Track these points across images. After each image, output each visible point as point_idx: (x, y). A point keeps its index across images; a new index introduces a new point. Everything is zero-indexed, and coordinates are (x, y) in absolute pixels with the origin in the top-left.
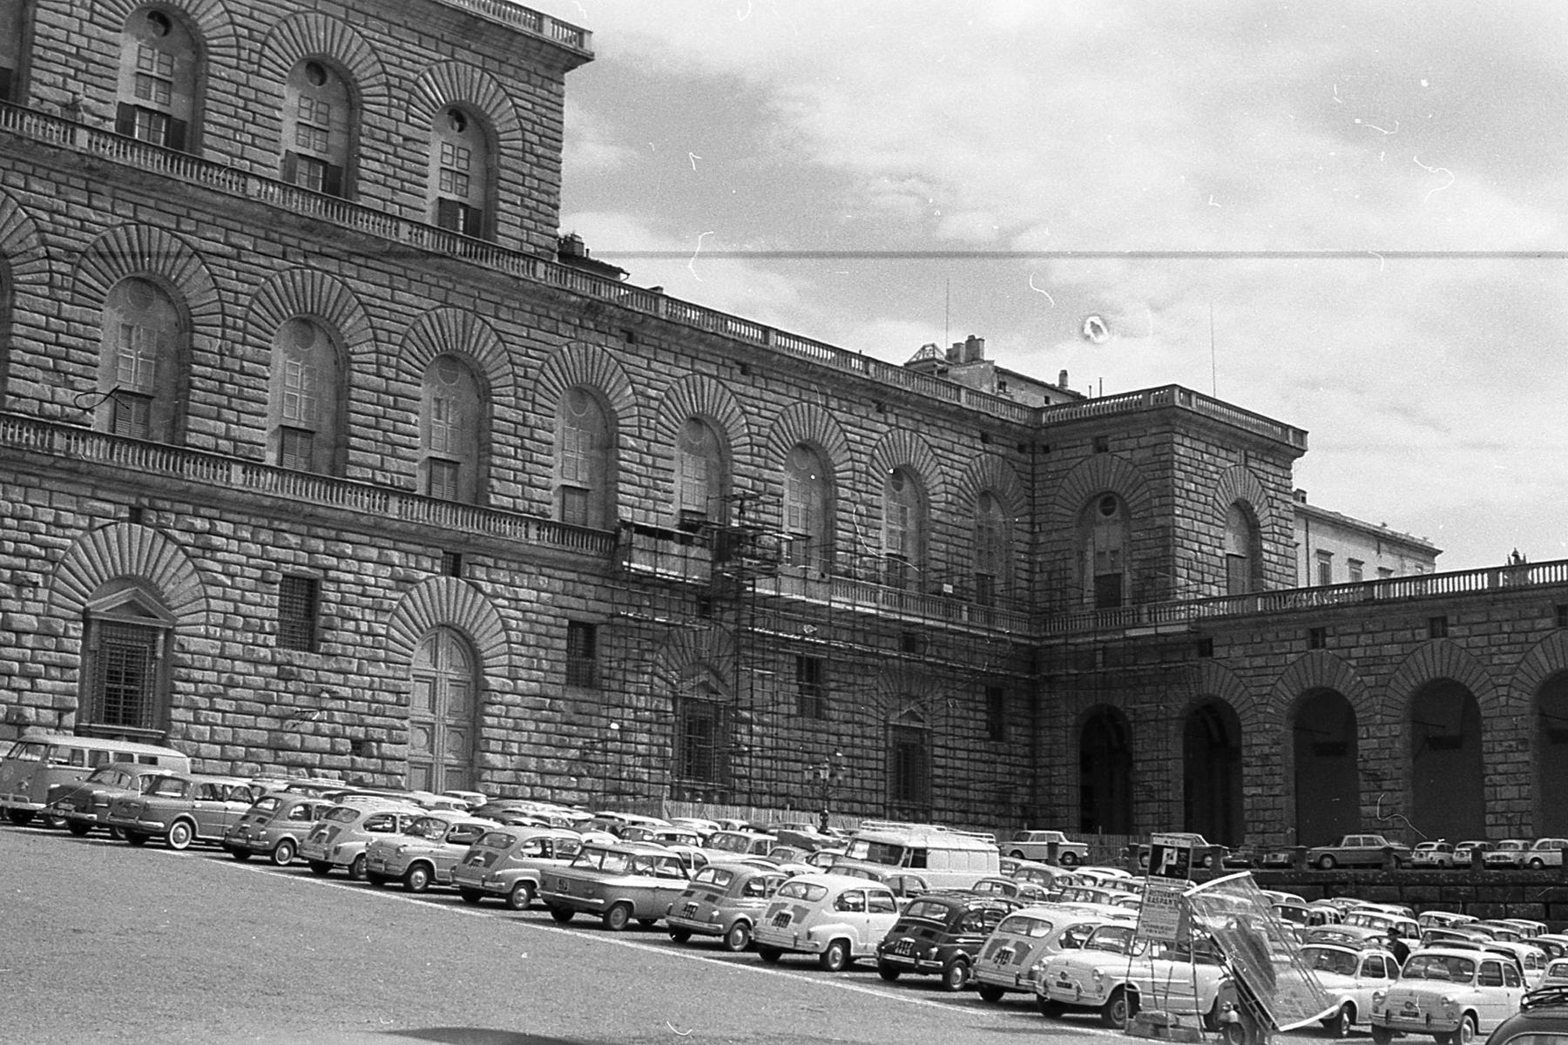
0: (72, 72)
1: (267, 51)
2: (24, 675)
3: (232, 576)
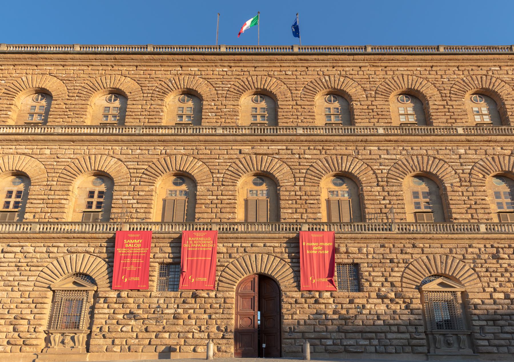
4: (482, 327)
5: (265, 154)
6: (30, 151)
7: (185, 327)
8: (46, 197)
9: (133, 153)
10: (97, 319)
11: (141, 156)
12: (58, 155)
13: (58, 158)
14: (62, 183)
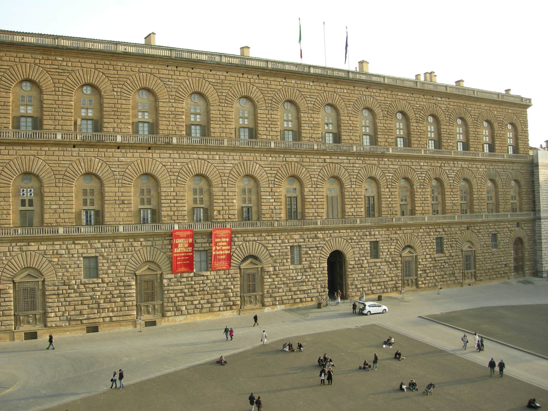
1: (478, 123)
2: (454, 264)
4: (421, 274)
5: (337, 163)
6: (205, 157)
7: (307, 286)
8: (223, 197)
10: (265, 285)
12: (225, 161)
13: (225, 163)
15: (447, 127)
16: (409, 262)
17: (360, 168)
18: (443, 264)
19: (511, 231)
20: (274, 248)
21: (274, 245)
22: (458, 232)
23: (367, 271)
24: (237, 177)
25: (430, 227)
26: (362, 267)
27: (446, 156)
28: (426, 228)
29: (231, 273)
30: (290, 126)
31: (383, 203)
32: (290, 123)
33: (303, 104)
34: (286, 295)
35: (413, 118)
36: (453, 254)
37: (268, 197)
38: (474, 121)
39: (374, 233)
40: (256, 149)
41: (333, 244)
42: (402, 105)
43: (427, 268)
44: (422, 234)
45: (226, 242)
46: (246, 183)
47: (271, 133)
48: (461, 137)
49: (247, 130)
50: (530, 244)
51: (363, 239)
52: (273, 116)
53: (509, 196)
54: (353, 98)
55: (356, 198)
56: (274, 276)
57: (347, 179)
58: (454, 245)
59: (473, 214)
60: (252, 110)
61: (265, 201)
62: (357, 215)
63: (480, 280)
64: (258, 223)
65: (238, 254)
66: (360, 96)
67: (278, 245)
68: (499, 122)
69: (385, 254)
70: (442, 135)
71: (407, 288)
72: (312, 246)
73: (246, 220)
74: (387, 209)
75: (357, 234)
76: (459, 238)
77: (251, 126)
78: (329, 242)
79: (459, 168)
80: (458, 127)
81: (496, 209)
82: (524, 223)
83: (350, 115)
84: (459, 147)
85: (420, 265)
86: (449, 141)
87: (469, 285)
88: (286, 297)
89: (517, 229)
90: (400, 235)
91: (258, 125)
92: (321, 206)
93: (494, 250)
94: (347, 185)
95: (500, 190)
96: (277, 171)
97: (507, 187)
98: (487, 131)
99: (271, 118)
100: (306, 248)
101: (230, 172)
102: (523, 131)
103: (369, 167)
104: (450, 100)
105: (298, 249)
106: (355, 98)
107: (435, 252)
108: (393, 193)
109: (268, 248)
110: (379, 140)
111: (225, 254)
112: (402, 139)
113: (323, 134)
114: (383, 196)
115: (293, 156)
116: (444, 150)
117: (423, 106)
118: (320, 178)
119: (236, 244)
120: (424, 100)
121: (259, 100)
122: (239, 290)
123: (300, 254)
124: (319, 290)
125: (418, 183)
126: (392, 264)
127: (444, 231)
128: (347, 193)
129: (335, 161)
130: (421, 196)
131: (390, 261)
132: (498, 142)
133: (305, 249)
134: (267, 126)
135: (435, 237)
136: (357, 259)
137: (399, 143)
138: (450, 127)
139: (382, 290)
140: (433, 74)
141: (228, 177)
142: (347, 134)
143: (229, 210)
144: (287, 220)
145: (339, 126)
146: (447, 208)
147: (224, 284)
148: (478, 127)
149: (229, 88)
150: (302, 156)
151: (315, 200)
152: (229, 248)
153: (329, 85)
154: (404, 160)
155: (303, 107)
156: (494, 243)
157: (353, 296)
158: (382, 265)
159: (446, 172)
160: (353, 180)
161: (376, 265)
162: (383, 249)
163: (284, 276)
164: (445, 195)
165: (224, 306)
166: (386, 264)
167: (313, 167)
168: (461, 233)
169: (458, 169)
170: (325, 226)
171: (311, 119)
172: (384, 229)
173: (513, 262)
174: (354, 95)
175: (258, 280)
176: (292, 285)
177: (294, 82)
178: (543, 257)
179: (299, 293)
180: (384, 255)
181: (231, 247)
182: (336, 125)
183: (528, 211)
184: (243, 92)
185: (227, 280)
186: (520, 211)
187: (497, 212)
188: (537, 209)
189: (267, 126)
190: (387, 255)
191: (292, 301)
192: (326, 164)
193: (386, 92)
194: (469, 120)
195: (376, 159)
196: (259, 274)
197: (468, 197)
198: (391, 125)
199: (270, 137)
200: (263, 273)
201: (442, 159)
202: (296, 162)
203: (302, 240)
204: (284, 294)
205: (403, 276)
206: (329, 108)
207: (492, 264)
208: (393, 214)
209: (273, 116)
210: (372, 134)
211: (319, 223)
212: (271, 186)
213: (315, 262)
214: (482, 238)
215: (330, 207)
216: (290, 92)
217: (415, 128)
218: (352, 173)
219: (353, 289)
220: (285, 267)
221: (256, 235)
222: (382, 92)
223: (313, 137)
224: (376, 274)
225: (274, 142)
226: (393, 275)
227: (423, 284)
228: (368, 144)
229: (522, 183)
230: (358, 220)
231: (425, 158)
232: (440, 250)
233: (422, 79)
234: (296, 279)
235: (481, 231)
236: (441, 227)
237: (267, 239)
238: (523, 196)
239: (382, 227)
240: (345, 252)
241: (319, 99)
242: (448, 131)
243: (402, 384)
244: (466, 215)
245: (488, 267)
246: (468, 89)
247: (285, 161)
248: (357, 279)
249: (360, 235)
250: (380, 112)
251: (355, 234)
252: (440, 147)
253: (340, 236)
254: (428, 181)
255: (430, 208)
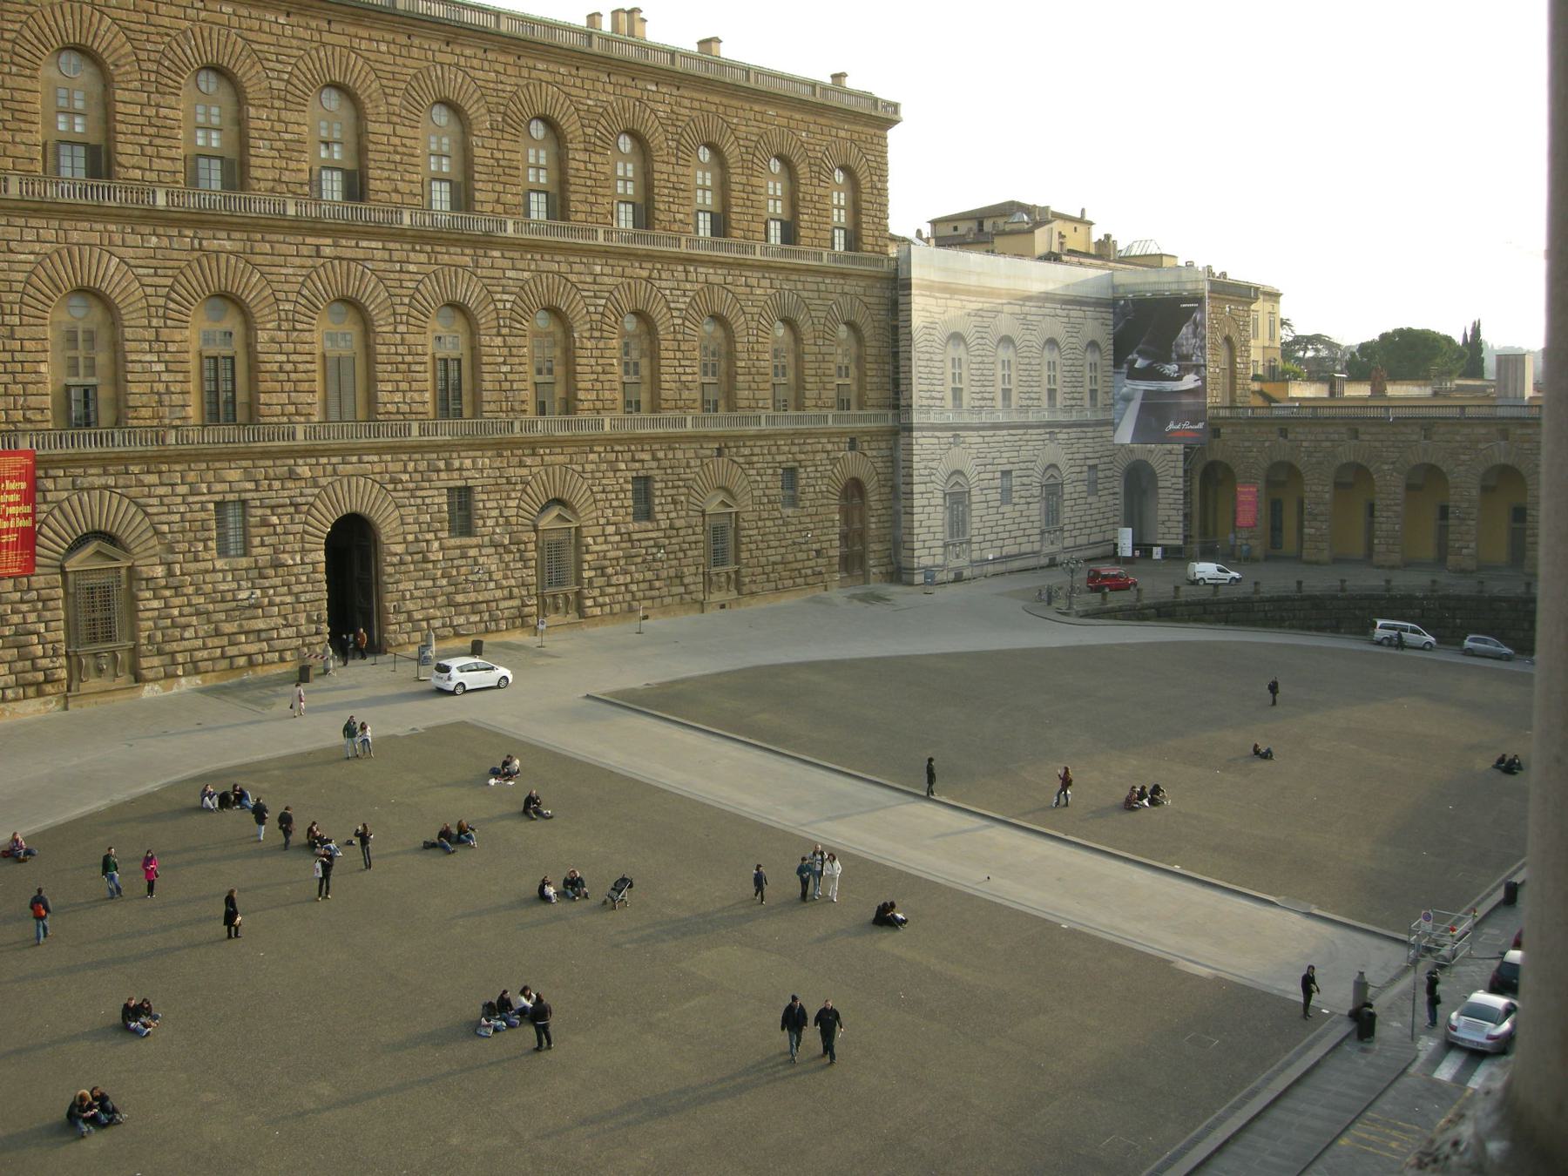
0: (671, 200)
1: (755, 160)
3: (761, 476)
4: (590, 578)
9: (145, 245)
10: (142, 620)
11: (159, 254)
13: (11, 251)
14: (32, 320)
15: (669, 168)
16: (558, 544)
17: (420, 277)
18: (650, 551)
19: (834, 461)
20: (165, 509)
21: (166, 500)
22: (692, 463)
23: (439, 573)
24: (50, 294)
25: (617, 448)
26: (426, 560)
27: (665, 249)
28: (605, 451)
29: (36, 586)
30: (215, 144)
31: (486, 377)
32: (214, 135)
33: (255, 80)
34: (205, 647)
35: (576, 137)
36: (679, 523)
37: (148, 357)
38: (745, 157)
39: (461, 464)
40: (109, 211)
41: (340, 496)
42: (547, 98)
43: (607, 563)
44: (593, 466)
45: (18, 491)
46: (79, 313)
47: (157, 163)
48: (707, 199)
49: (81, 151)
50: (884, 497)
51: (430, 481)
52: (163, 112)
53: (832, 366)
54: (405, 71)
55: (409, 364)
56: (167, 593)
57: (382, 307)
58: (683, 498)
59: (734, 414)
60: (97, 89)
61: (138, 367)
62: (411, 413)
63: (752, 594)
64: (116, 435)
65: (58, 528)
66: (426, 64)
67: (179, 500)
68: (812, 161)
69: (490, 522)
70: (656, 191)
71: (553, 618)
72: (281, 501)
73: (78, 426)
74: (495, 396)
75: (411, 466)
76: (694, 480)
77: (95, 138)
78: (330, 490)
79: (700, 286)
80: (699, 169)
81: (797, 399)
82: (869, 438)
83: (395, 119)
84: (701, 224)
85: (587, 552)
86: (674, 208)
87: (723, 606)
88: (205, 654)
89: (849, 454)
90: (534, 470)
91: (115, 137)
92: (305, 386)
93: (789, 511)
94: (383, 325)
95: (807, 349)
96: (175, 277)
97: (827, 342)
98: (779, 186)
99: (157, 115)
100: (261, 507)
101: (29, 278)
102: (875, 192)
103: (446, 273)
104: (683, 92)
105: (239, 511)
106: (411, 71)
107: (630, 518)
108: (514, 351)
109: (150, 510)
110: (478, 195)
111: (16, 530)
112: (543, 197)
113: (314, 173)
114: (485, 359)
115: (223, 235)
116: (658, 232)
117: (605, 104)
118: (303, 301)
119: (49, 499)
120: (610, 88)
121: (119, 59)
122: (62, 635)
123: (245, 527)
124: (303, 630)
125: (586, 323)
126: (511, 552)
127: (654, 458)
128: (383, 349)
129: (348, 253)
130: (593, 362)
131: (506, 542)
132: (806, 217)
133: (259, 512)
134: (145, 140)
135: (630, 475)
136: (410, 538)
137: (534, 206)
138: (679, 170)
139: (483, 625)
140: (636, 16)
141: (23, 293)
142: (386, 174)
143: (25, 394)
144: (204, 426)
145: (361, 151)
146: (664, 394)
147: (16, 619)
148: (755, 173)
149: (24, 17)
150: (252, 236)
151: (289, 367)
152: (28, 509)
153: (335, 27)
154: (547, 257)
155: (257, 88)
156: (790, 492)
157: (400, 645)
158: (481, 555)
159: (664, 295)
160: (400, 309)
161: (464, 556)
162: (484, 508)
163: (198, 592)
164: (660, 358)
165: (18, 685)
166: (492, 550)
167: (284, 271)
168: (702, 465)
169: (697, 287)
170: (318, 442)
171: (279, 126)
172: (489, 454)
173: (837, 543)
174: (409, 62)
175: (119, 603)
176: (222, 616)
177: (230, 10)
178: (916, 531)
179: (243, 638)
180: (488, 523)
181: (34, 509)
182: (352, 146)
183: (879, 407)
184: (70, 31)
185: (24, 607)
186: (860, 408)
187: (798, 409)
188: (902, 402)
189: (145, 140)
190: (497, 525)
191: (224, 664)
192: (322, 261)
193: (502, 58)
194: (732, 151)
195: (467, 251)
196: (124, 586)
197: (723, 364)
198: (513, 156)
199: (153, 176)
200: (135, 583)
201: (654, 257)
202: (231, 253)
203: (251, 486)
204: (200, 643)
205: (541, 585)
206: (334, 95)
207: (783, 550)
208: (513, 410)
209: (163, 112)
210: (458, 178)
211: (300, 435)
212: (155, 322)
213: (288, 548)
214: (759, 478)
215: (333, 387)
216: (215, 42)
217: (582, 166)
218: (398, 291)
219: (399, 624)
220: (201, 566)
221: (111, 469)
222: (490, 56)
223: (284, 179)
224: (466, 580)
225: (164, 191)
226: (513, 582)
227: (596, 605)
228: (446, 207)
229: (867, 332)
230: (415, 427)
231: (606, 253)
232: (644, 512)
233: (606, 26)
234: (234, 600)
235: (755, 459)
236: (647, 447)
237: (146, 482)
238: (868, 366)
239: (482, 447)
240: (377, 518)
241: (304, 69)
242: (674, 178)
243: (544, 883)
244: (715, 414)
245: (772, 559)
246: (733, 66)
247: (200, 250)
248: (411, 594)
249: (420, 469)
250: (481, 116)
251: (405, 466)
252: (648, 225)
253: (361, 472)
254: (613, 319)
255: (619, 396)
